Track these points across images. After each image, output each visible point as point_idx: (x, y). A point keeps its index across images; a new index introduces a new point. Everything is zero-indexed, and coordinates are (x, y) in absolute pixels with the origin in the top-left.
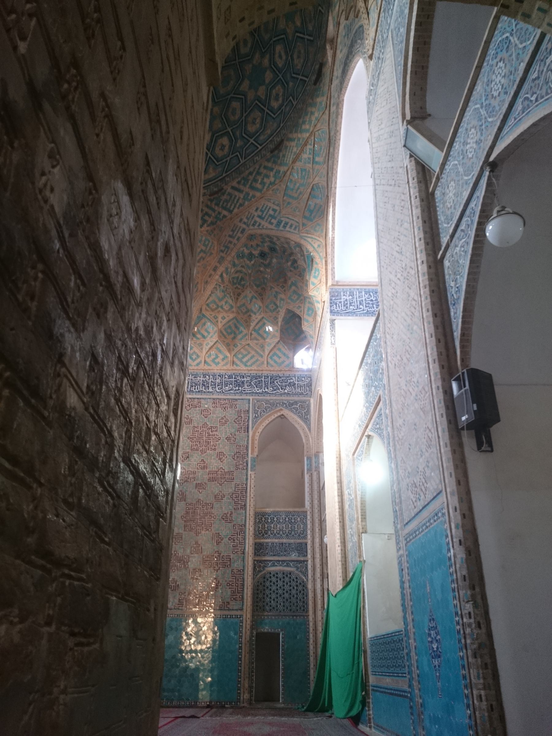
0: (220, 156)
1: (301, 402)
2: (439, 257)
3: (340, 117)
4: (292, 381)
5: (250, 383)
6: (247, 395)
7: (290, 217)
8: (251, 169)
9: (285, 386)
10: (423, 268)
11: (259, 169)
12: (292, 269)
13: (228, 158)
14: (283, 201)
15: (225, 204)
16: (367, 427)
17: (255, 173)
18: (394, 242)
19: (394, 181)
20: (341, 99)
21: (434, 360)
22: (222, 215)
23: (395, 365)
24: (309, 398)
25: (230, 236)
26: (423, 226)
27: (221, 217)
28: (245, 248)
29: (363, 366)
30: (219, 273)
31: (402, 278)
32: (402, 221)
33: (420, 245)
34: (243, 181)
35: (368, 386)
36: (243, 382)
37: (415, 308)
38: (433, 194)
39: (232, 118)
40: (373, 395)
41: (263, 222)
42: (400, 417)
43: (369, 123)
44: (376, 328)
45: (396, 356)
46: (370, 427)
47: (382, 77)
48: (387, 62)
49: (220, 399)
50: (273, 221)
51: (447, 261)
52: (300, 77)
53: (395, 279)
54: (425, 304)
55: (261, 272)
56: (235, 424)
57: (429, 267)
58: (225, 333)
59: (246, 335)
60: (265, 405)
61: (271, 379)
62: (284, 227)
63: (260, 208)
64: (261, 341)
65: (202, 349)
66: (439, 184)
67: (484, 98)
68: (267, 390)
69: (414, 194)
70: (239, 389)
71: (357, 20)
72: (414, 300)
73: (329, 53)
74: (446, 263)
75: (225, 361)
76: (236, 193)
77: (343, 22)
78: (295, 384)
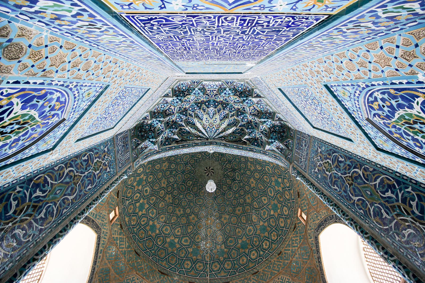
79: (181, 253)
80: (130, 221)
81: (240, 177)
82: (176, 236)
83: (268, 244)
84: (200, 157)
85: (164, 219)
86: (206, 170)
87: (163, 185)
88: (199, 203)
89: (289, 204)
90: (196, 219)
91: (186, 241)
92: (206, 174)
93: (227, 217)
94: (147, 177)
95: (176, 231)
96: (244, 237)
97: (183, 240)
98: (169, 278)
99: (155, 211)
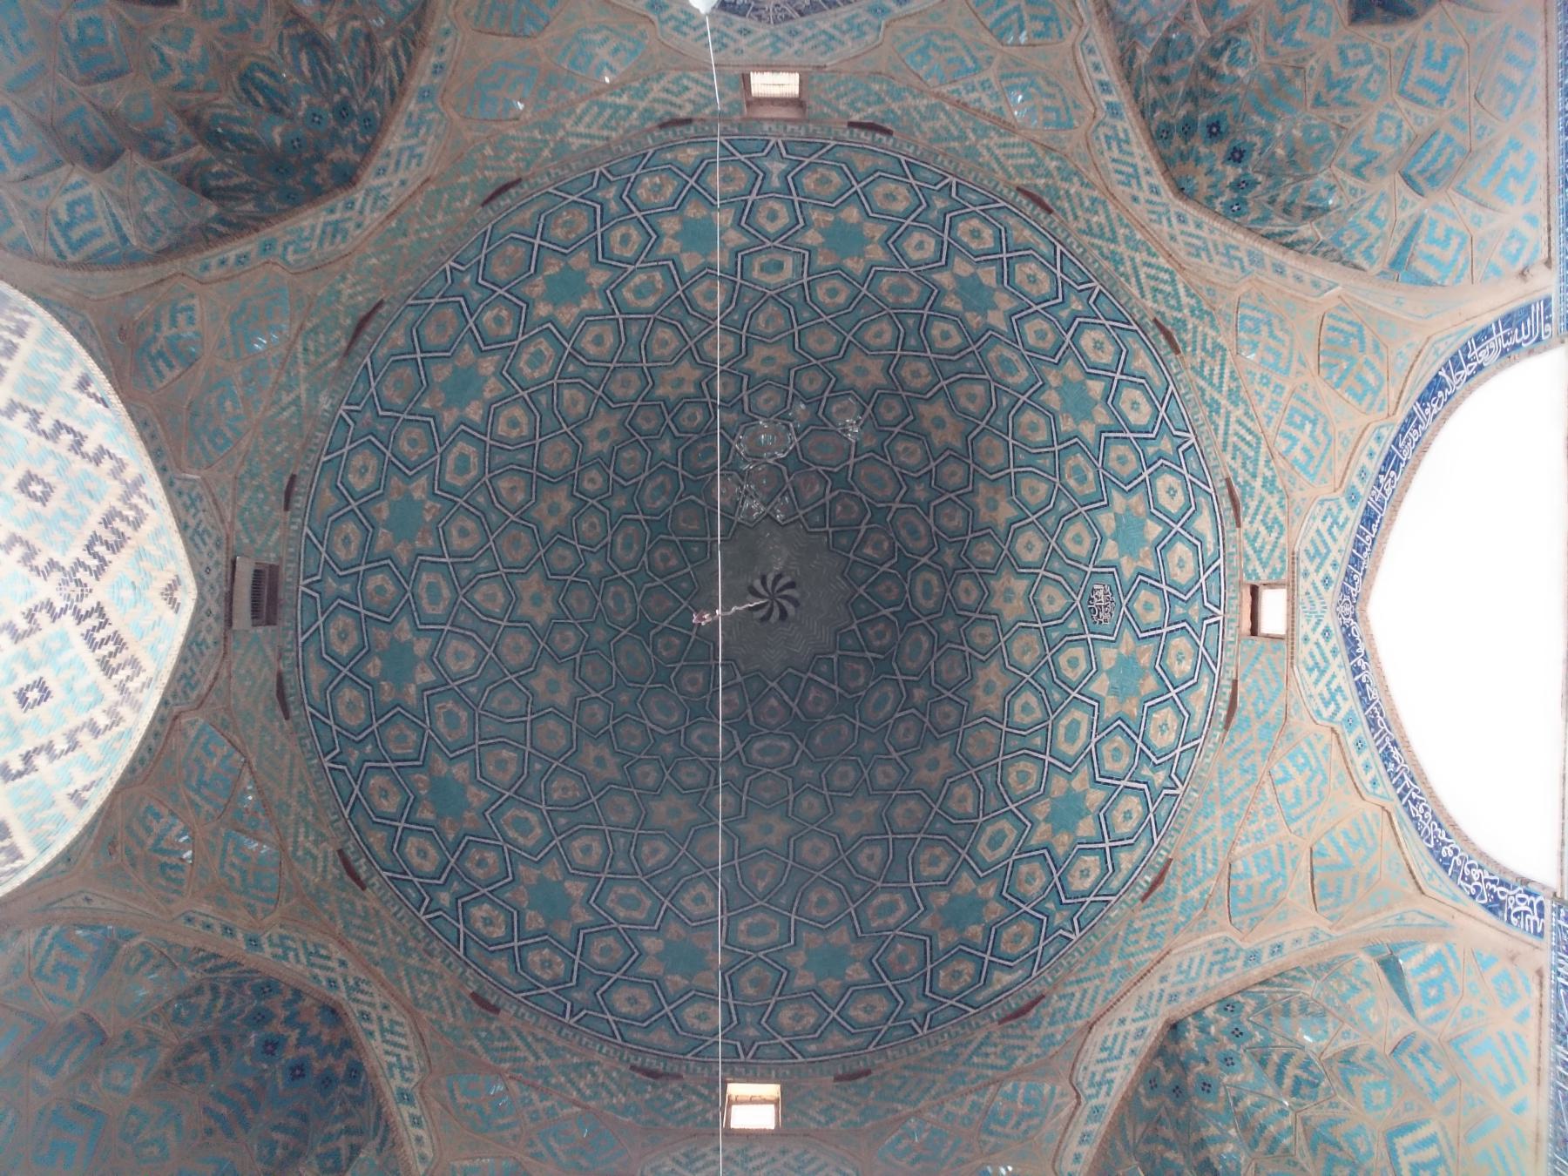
8: (1096, 252)
28: (1217, 202)
41: (1141, 165)
76: (1143, 276)
79: (416, 433)
80: (674, 170)
81: (768, 760)
82: (492, 411)
83: (499, 932)
84: (868, 551)
85: (592, 350)
86: (783, 582)
87: (760, 352)
88: (619, 540)
89: (752, 1032)
90: (550, 524)
91: (462, 466)
92: (757, 583)
93: (563, 699)
94: (848, 278)
95: (518, 412)
96: (484, 795)
97: (470, 449)
98: (334, 364)
99: (650, 302)
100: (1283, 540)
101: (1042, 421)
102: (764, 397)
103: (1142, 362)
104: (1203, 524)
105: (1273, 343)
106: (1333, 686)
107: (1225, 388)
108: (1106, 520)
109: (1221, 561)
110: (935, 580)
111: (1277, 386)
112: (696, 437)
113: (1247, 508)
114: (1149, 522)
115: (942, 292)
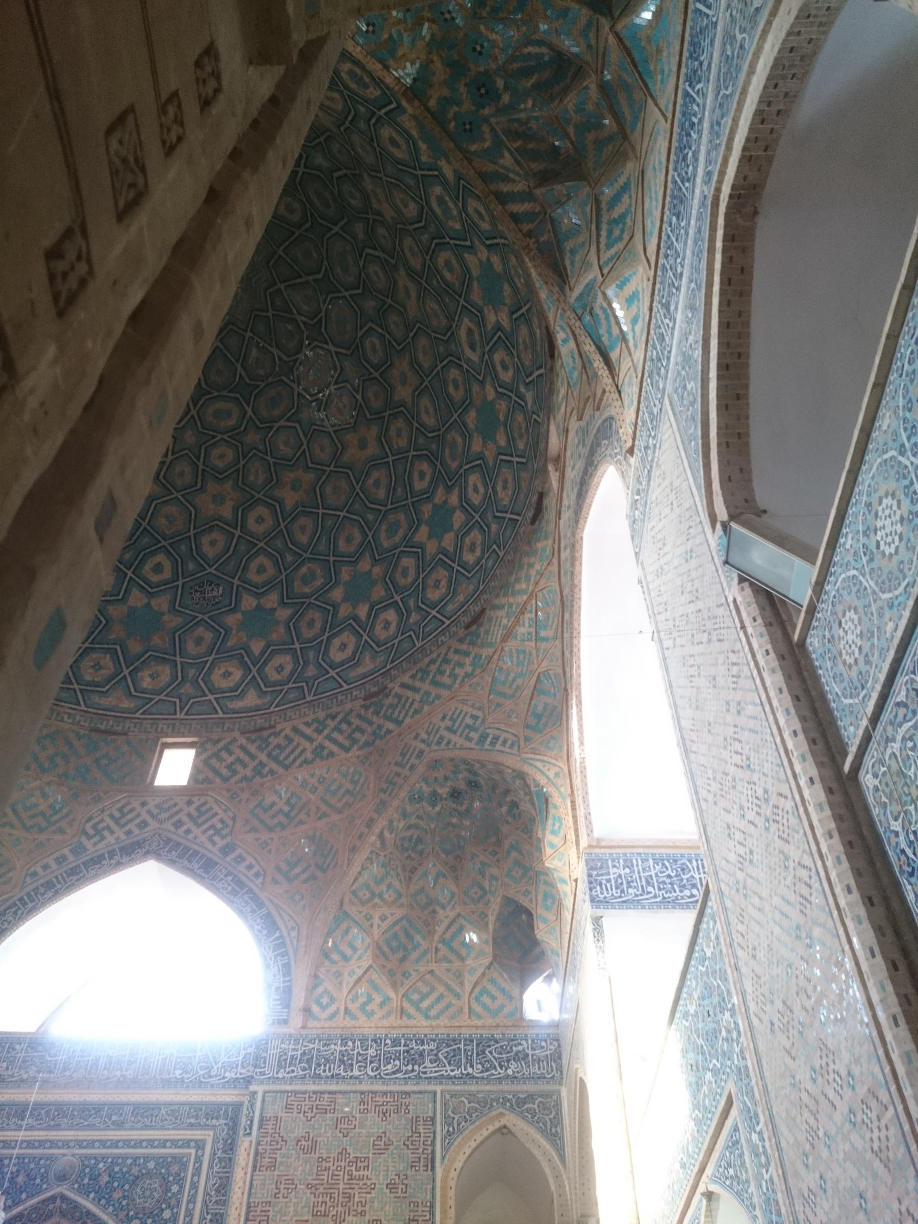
0: (382, 638)
1: (541, 1096)
2: (847, 767)
3: (577, 563)
4: (520, 1048)
5: (436, 1055)
6: (429, 1083)
7: (502, 727)
9: (508, 1061)
10: (815, 795)
11: (446, 654)
12: (510, 819)
13: (396, 641)
14: (489, 701)
15: (390, 711)
16: (702, 1170)
17: (440, 660)
18: (725, 748)
19: (706, 634)
20: (577, 537)
21: (895, 1018)
22: (384, 730)
23: (772, 1024)
24: (558, 1087)
25: (397, 764)
26: (794, 706)
27: (382, 733)
28: (423, 784)
29: (676, 1020)
30: (377, 831)
31: (760, 822)
32: (739, 704)
33: (797, 745)
34: (419, 675)
35: (694, 1068)
36: (421, 1054)
37: (810, 887)
38: (802, 644)
39: (402, 582)
40: (710, 1090)
41: (455, 738)
42: (807, 1166)
43: (636, 553)
44: (701, 934)
45: (772, 1002)
46: (709, 1170)
47: (656, 473)
48: (665, 446)
49: (375, 1093)
50: (472, 734)
51: (869, 776)
52: (508, 516)
53: (742, 825)
54: (838, 875)
55: (454, 826)
56: (406, 1151)
57: (830, 791)
58: (385, 949)
59: (426, 952)
60: (468, 1105)
61: (478, 1045)
62: (493, 744)
63: (450, 714)
64: (457, 964)
65: (341, 983)
66: (815, 624)
67: (904, 436)
68: (470, 1070)
69: (760, 647)
70: (413, 1070)
71: (597, 413)
72: (804, 867)
73: (554, 476)
74: (868, 780)
75: (386, 1009)
76: (409, 693)
77: (574, 425)
78: (527, 1055)
84: (254, 353)
100: (218, 780)
101: (352, 549)
102: (381, 274)
103: (368, 665)
104: (252, 699)
105: (343, 790)
106: (106, 833)
107: (327, 743)
108: (272, 600)
109: (221, 715)
110: (232, 422)
111: (316, 789)
112: (336, 194)
113: (253, 742)
114: (262, 644)
115: (449, 489)
